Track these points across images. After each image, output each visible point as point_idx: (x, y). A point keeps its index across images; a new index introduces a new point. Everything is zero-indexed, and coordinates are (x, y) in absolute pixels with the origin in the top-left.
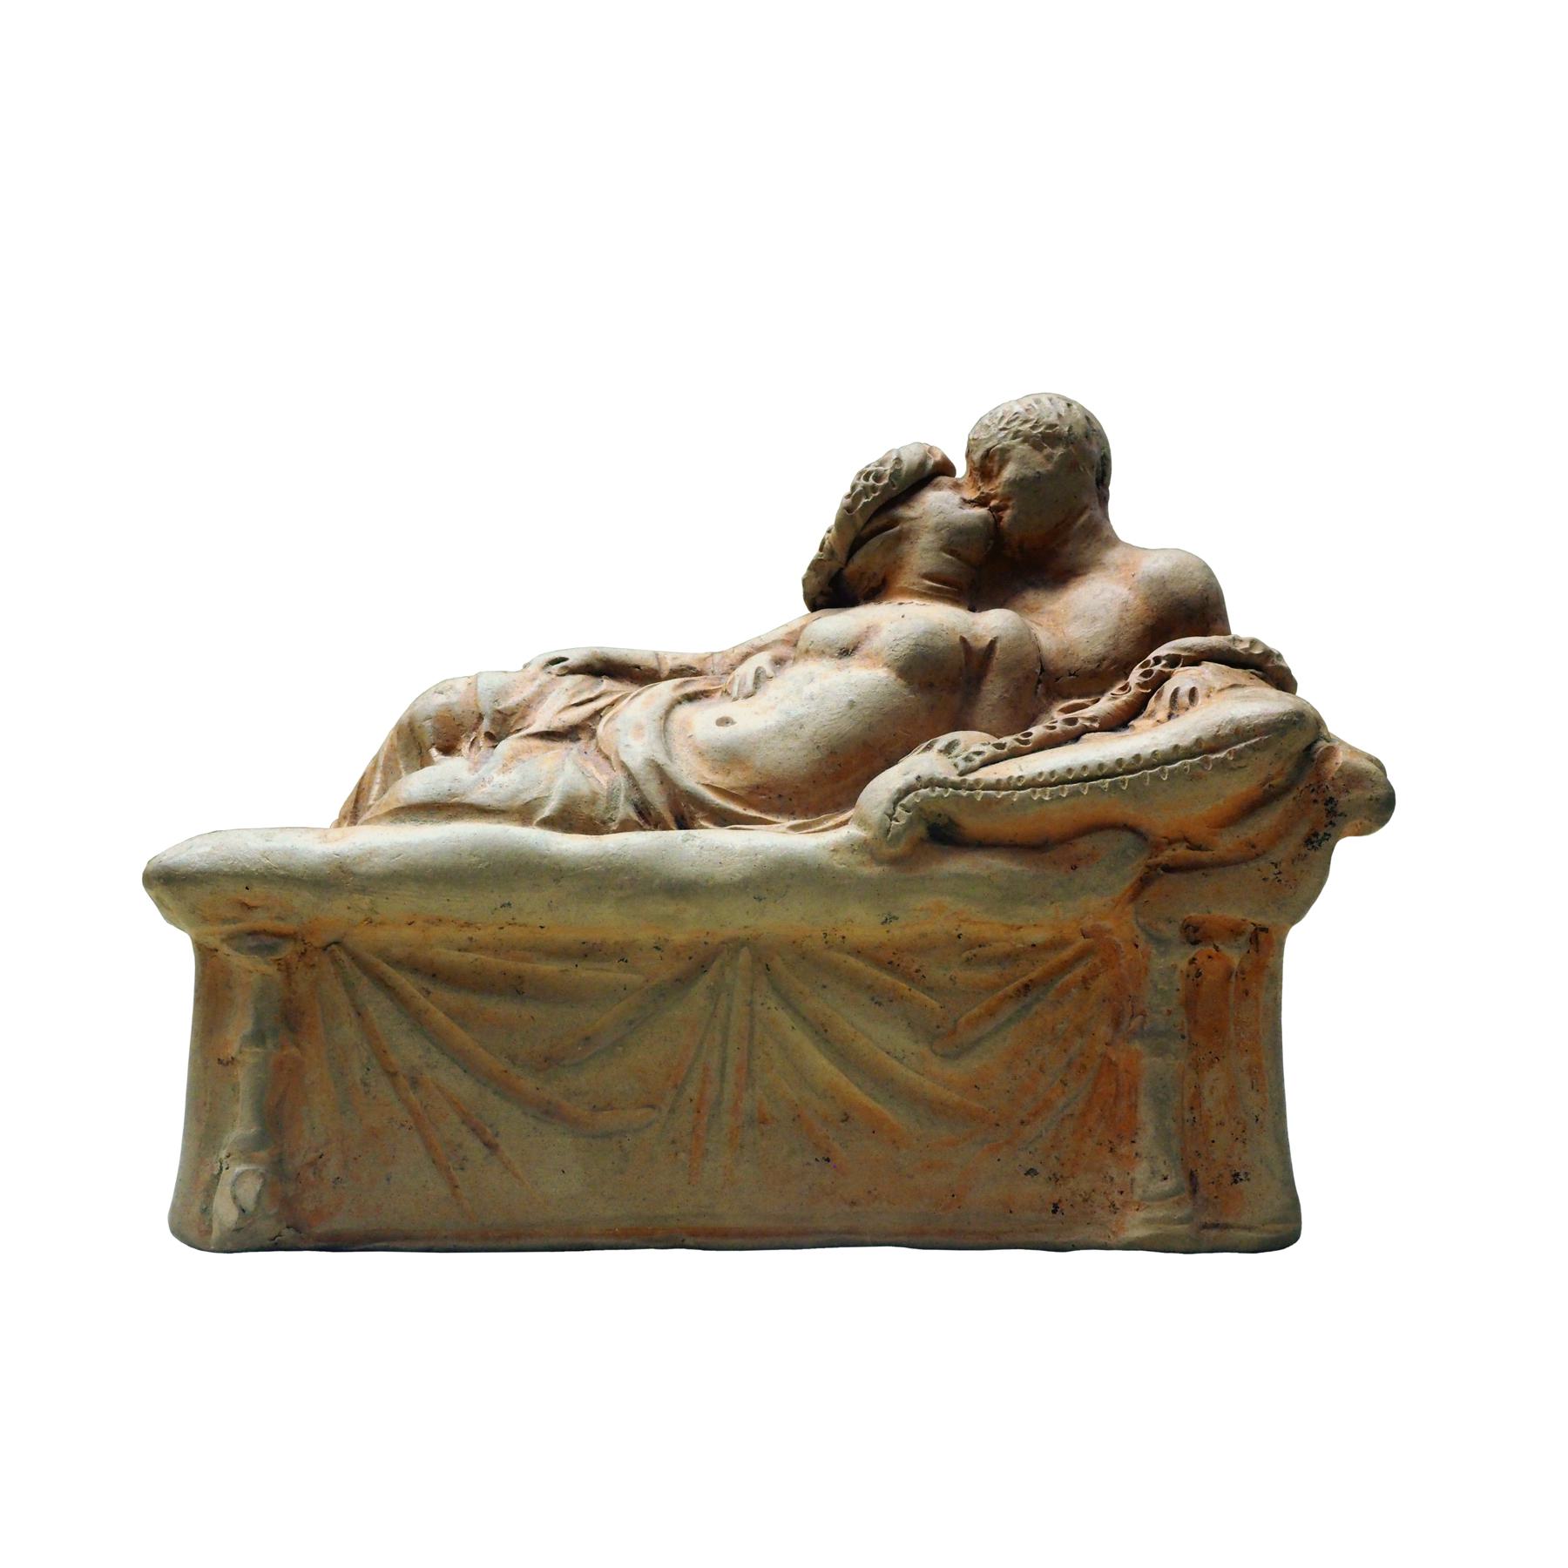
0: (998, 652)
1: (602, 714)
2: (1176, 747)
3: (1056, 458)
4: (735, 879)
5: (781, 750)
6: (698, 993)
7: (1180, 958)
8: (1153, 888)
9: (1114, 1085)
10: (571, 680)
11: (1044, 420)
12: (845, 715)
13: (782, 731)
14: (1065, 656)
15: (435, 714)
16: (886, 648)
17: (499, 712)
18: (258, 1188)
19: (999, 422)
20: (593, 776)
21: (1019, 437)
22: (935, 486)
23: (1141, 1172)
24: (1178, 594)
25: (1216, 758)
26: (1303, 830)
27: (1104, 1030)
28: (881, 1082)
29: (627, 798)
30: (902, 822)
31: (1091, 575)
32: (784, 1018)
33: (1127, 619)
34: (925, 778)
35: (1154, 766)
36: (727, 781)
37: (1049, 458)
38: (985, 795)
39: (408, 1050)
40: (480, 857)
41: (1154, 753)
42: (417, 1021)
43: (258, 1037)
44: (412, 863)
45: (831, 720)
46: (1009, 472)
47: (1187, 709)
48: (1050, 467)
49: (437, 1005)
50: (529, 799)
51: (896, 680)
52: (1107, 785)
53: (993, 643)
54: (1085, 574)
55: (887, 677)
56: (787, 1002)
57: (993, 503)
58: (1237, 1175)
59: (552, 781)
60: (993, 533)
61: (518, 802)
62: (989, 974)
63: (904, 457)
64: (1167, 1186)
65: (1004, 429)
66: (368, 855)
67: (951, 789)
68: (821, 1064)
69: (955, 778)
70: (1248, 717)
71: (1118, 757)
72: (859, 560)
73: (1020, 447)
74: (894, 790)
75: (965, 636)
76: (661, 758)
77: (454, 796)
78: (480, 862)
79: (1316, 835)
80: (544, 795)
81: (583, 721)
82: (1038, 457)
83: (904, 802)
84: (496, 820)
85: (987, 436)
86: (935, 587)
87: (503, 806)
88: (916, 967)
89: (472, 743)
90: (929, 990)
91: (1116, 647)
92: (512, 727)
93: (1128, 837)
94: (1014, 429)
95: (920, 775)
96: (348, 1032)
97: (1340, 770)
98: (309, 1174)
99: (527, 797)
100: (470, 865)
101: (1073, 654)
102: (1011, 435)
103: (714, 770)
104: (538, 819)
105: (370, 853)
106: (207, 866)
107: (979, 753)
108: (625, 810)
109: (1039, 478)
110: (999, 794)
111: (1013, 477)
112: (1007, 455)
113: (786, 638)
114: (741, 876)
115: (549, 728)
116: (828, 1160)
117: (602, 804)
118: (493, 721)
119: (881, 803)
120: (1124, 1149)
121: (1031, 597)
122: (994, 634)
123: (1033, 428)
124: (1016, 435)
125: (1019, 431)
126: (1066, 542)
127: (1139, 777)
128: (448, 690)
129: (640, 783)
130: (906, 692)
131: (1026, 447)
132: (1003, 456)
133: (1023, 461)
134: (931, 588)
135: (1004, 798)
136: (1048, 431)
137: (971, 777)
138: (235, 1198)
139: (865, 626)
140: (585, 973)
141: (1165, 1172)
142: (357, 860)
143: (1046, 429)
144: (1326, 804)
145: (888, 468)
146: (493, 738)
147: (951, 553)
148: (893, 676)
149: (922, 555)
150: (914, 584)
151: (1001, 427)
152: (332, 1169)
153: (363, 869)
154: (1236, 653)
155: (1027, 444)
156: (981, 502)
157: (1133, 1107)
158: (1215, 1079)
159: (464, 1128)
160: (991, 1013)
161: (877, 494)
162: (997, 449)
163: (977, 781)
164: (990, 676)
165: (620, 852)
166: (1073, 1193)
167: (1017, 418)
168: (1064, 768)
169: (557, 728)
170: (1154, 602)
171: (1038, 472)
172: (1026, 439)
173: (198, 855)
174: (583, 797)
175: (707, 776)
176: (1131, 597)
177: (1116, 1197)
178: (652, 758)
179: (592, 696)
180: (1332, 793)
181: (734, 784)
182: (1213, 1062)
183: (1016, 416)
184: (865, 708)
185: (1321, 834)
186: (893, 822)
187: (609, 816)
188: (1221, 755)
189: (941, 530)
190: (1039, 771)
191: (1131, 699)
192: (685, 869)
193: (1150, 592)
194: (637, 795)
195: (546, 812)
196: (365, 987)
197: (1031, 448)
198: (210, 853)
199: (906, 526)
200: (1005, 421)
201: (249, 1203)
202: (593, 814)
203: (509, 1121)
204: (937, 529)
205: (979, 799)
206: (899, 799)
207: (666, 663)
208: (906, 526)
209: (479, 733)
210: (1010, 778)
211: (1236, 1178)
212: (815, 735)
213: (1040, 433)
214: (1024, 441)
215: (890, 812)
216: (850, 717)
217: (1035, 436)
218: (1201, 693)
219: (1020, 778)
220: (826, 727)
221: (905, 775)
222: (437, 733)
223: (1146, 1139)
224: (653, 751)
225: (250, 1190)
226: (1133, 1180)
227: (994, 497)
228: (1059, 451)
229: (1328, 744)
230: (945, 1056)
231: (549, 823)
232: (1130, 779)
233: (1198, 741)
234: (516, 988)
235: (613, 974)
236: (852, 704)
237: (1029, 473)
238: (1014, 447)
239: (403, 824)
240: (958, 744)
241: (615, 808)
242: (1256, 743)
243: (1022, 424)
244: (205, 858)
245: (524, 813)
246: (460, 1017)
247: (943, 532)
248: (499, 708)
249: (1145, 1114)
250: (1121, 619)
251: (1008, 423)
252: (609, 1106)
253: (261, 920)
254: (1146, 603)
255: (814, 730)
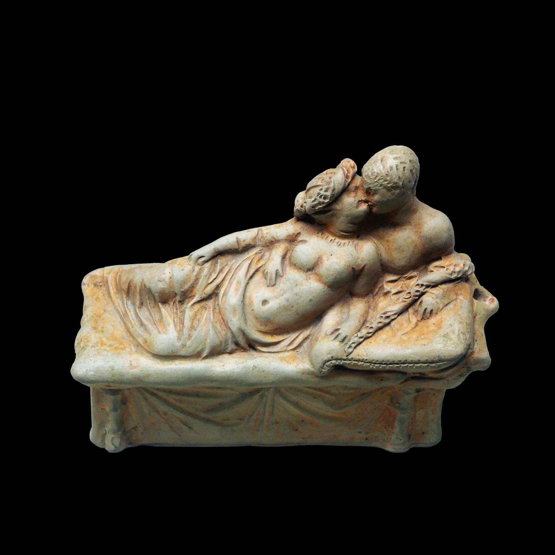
0: (365, 269)
1: (219, 286)
2: (419, 360)
3: (396, 194)
4: (270, 382)
5: (285, 315)
6: (257, 397)
7: (414, 395)
8: (408, 382)
9: (388, 414)
10: (208, 265)
11: (393, 181)
12: (308, 304)
13: (285, 308)
14: (391, 263)
15: (159, 292)
16: (324, 277)
17: (182, 292)
18: (120, 441)
19: (375, 178)
20: (220, 332)
21: (382, 186)
22: (348, 191)
23: (393, 437)
24: (436, 244)
25: (432, 366)
26: (459, 373)
27: (387, 401)
28: (314, 414)
29: (232, 342)
30: (326, 370)
31: (405, 227)
32: (284, 402)
33: (415, 252)
34: (334, 358)
35: (411, 363)
36: (266, 329)
37: (393, 194)
38: (354, 363)
39: (163, 408)
40: (185, 379)
41: (412, 360)
42: (166, 402)
43: (115, 409)
44: (163, 381)
45: (303, 306)
46: (376, 198)
47: (428, 319)
48: (393, 197)
49: (172, 398)
50: (199, 350)
51: (327, 289)
52: (395, 367)
53: (364, 267)
54: (402, 226)
55: (324, 288)
56: (285, 398)
57: (369, 203)
58: (424, 433)
59: (206, 339)
60: (369, 213)
61: (195, 352)
62: (351, 391)
63: (336, 187)
64: (401, 442)
65: (376, 182)
66: (148, 376)
67: (343, 361)
68: (295, 411)
69: (345, 358)
70: (444, 356)
71: (400, 360)
72: (316, 217)
73: (382, 190)
74: (324, 360)
75: (354, 267)
76: (244, 327)
77: (174, 353)
78: (185, 380)
79: (462, 374)
80: (204, 347)
81: (213, 292)
82: (389, 194)
83: (327, 364)
84: (188, 359)
85: (370, 182)
86: (346, 235)
87: (190, 355)
88: (328, 390)
89: (174, 302)
90: (332, 394)
91: (410, 262)
92: (187, 296)
93: (399, 376)
94: (381, 183)
95: (333, 357)
96: (143, 403)
97: (474, 360)
98: (133, 431)
99: (199, 349)
100: (182, 381)
101: (394, 263)
102: (379, 185)
103: (261, 325)
104: (202, 357)
105: (148, 376)
106: (94, 379)
107: (353, 343)
108: (231, 346)
109: (388, 201)
110: (358, 363)
111: (378, 200)
112: (377, 192)
113: (286, 238)
114: (271, 381)
115: (201, 298)
116: (297, 430)
117: (223, 344)
118: (181, 296)
119: (319, 363)
120: (390, 429)
121: (381, 232)
122: (365, 262)
123: (388, 184)
124: (381, 185)
125: (383, 184)
126: (397, 214)
127: (406, 366)
128: (163, 281)
129: (237, 337)
130: (330, 292)
131: (384, 190)
132: (376, 192)
133: (383, 195)
134: (343, 235)
135: (360, 365)
136: (394, 185)
137: (350, 357)
138: (113, 444)
139: (317, 257)
140: (219, 391)
141: (401, 438)
142: (144, 377)
143: (393, 184)
144: (467, 368)
145: (329, 194)
146: (181, 302)
147: (352, 224)
148: (326, 287)
149: (341, 223)
150: (337, 232)
151: (375, 181)
152: (141, 430)
153: (147, 380)
154: (451, 279)
155: (385, 189)
156: (366, 202)
157: (394, 421)
158: (420, 414)
159: (182, 424)
160: (352, 399)
161: (324, 205)
162: (373, 189)
163: (352, 358)
164: (362, 276)
165: (232, 375)
166: (372, 436)
167: (383, 178)
168: (381, 360)
169: (204, 297)
170: (426, 246)
171: (388, 199)
172: (385, 187)
173: (91, 375)
174: (217, 345)
175: (259, 327)
176: (418, 243)
177: (385, 438)
178: (240, 327)
179: (215, 277)
180: (469, 365)
181: (268, 329)
182: (421, 409)
183: (382, 177)
184: (316, 301)
185: (464, 374)
186: (323, 369)
187: (226, 348)
188: (434, 365)
189: (348, 217)
190: (373, 359)
191: (410, 302)
192: (253, 380)
193: (425, 243)
194: (235, 339)
195: (205, 354)
196: (148, 396)
197: (386, 190)
198: (94, 375)
199: (335, 212)
200: (378, 178)
201: (117, 444)
202: (221, 349)
203: (195, 423)
204: (347, 216)
205: (352, 364)
206: (325, 363)
207: (241, 244)
208: (335, 212)
209: (176, 299)
210: (363, 359)
211: (423, 433)
212: (297, 310)
213: (391, 186)
214: (383, 188)
215: (322, 367)
216: (310, 305)
217: (389, 187)
218: (434, 312)
219: (366, 360)
220: (301, 308)
221: (328, 354)
222: (160, 298)
223: (397, 430)
224: (240, 324)
225: (117, 442)
226: (391, 438)
227: (371, 202)
228: (398, 191)
229: (472, 351)
230: (336, 409)
231: (206, 357)
232: (403, 366)
233: (427, 360)
234: (197, 395)
235: (228, 392)
236: (311, 300)
237: (385, 199)
238: (380, 190)
239: (157, 359)
240: (347, 337)
241: (228, 345)
242: (446, 363)
243: (384, 182)
244: (93, 377)
245: (196, 355)
246: (180, 401)
247: (349, 217)
248: (182, 290)
249: (397, 424)
250: (413, 252)
251: (378, 180)
252: (228, 419)
253: (112, 388)
254: (423, 246)
255: (297, 308)
